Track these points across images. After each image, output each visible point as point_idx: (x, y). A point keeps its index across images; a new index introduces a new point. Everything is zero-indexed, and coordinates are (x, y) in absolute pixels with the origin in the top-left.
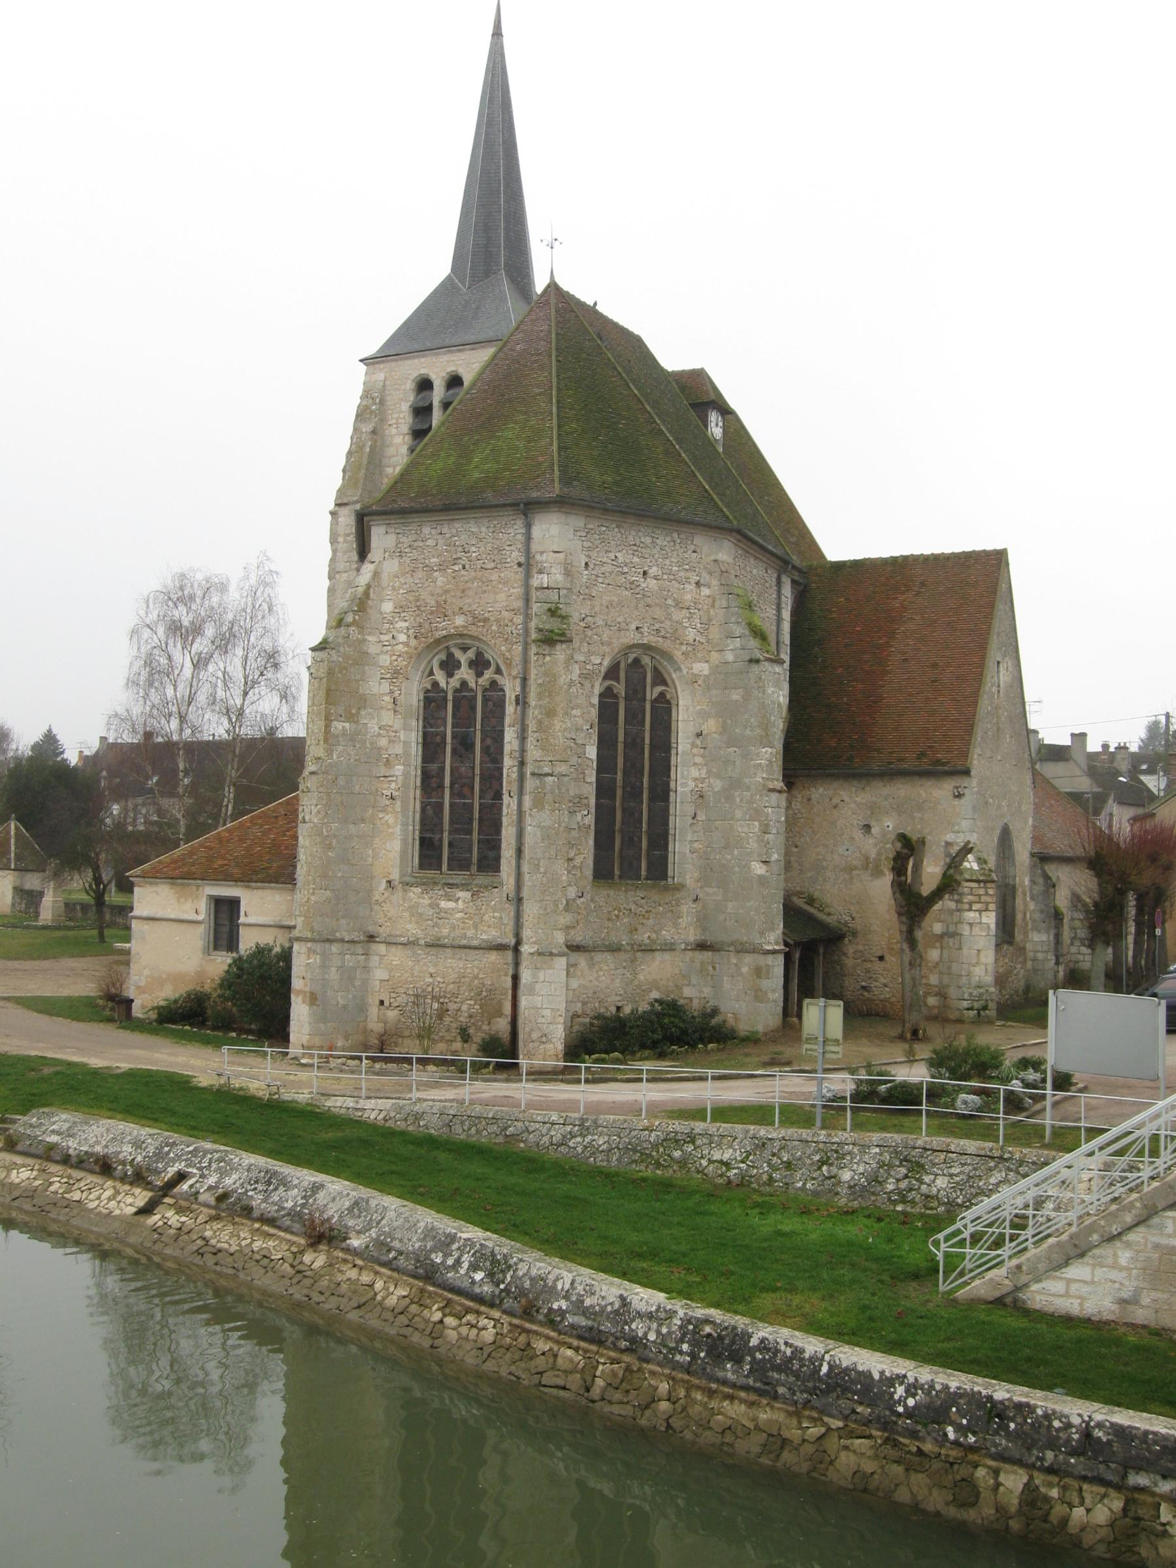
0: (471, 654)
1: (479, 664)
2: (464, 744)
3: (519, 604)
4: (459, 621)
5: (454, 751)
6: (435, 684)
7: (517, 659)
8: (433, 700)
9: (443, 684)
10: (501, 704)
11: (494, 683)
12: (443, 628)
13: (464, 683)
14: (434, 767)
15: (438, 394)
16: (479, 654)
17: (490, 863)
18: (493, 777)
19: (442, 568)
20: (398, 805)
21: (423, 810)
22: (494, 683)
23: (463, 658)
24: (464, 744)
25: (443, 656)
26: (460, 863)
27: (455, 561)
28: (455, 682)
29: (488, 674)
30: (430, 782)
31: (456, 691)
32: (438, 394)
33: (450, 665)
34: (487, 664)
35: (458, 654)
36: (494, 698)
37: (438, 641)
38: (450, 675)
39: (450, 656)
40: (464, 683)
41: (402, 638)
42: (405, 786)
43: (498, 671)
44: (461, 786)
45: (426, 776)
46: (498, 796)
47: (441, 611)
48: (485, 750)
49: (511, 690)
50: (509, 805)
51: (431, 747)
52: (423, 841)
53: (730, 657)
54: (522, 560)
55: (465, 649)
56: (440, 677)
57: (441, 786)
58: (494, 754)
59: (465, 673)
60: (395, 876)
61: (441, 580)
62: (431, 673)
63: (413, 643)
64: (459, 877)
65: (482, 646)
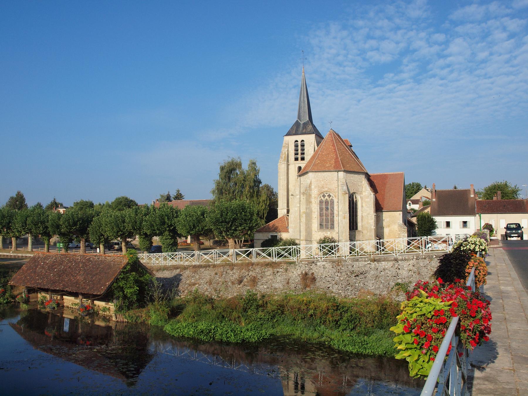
0: (328, 194)
1: (329, 196)
2: (327, 209)
3: (337, 186)
4: (326, 189)
5: (325, 210)
6: (321, 199)
7: (337, 195)
8: (321, 202)
10: (333, 202)
11: (332, 199)
12: (323, 190)
13: (327, 199)
14: (322, 212)
15: (299, 144)
16: (329, 194)
17: (332, 227)
18: (332, 214)
19: (323, 180)
20: (316, 218)
21: (320, 219)
22: (332, 199)
23: (326, 195)
24: (327, 209)
25: (323, 195)
27: (325, 179)
28: (325, 199)
29: (331, 198)
30: (321, 215)
31: (331, 200)
32: (299, 144)
33: (324, 196)
34: (331, 196)
35: (325, 194)
36: (332, 202)
37: (322, 192)
38: (324, 198)
39: (324, 194)
40: (327, 199)
41: (316, 192)
42: (317, 215)
43: (333, 197)
44: (327, 215)
45: (320, 214)
46: (333, 217)
47: (323, 187)
48: (331, 210)
49: (335, 200)
50: (336, 218)
51: (321, 209)
52: (320, 224)
53: (367, 194)
54: (337, 179)
55: (327, 193)
56: (323, 198)
57: (323, 216)
58: (332, 211)
59: (327, 197)
60: (316, 230)
61: (322, 182)
62: (321, 197)
63: (318, 193)
64: (327, 230)
65: (330, 193)
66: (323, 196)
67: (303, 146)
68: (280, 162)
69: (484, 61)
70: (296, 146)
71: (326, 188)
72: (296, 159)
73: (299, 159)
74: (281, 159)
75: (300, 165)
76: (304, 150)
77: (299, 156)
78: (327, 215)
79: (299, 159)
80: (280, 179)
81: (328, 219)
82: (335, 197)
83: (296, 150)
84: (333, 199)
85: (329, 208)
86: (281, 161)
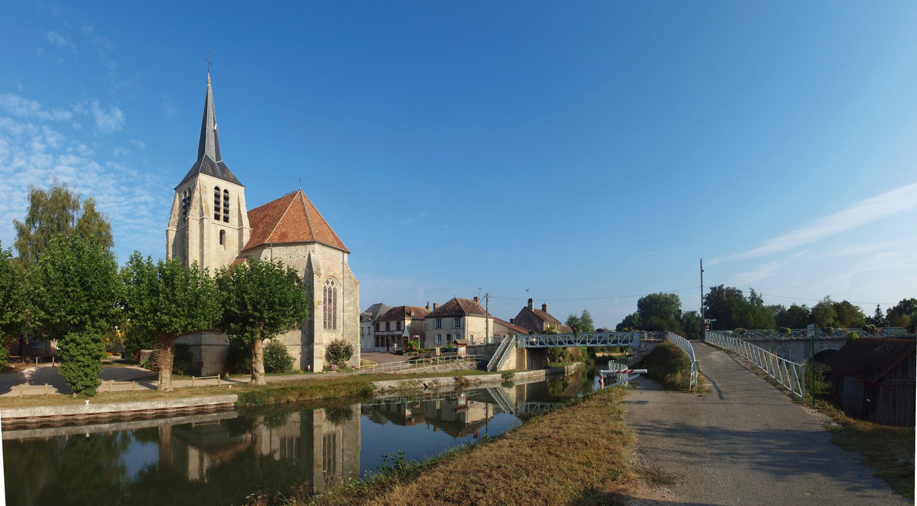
2: (330, 300)
3: (342, 272)
4: (332, 273)
9: (327, 286)
17: (335, 327)
18: (335, 308)
24: (330, 300)
26: (330, 327)
32: (222, 194)
35: (329, 280)
44: (330, 310)
46: (336, 313)
57: (326, 310)
58: (335, 304)
59: (330, 284)
61: (329, 263)
66: (326, 282)
67: (226, 198)
68: (192, 215)
69: (19, 170)
70: (217, 196)
71: (332, 271)
72: (217, 217)
73: (222, 218)
74: (193, 210)
75: (223, 228)
76: (228, 206)
77: (222, 214)
78: (330, 310)
79: (222, 218)
80: (192, 244)
81: (331, 314)
82: (340, 285)
83: (217, 203)
84: (337, 288)
85: (332, 299)
86: (194, 214)
